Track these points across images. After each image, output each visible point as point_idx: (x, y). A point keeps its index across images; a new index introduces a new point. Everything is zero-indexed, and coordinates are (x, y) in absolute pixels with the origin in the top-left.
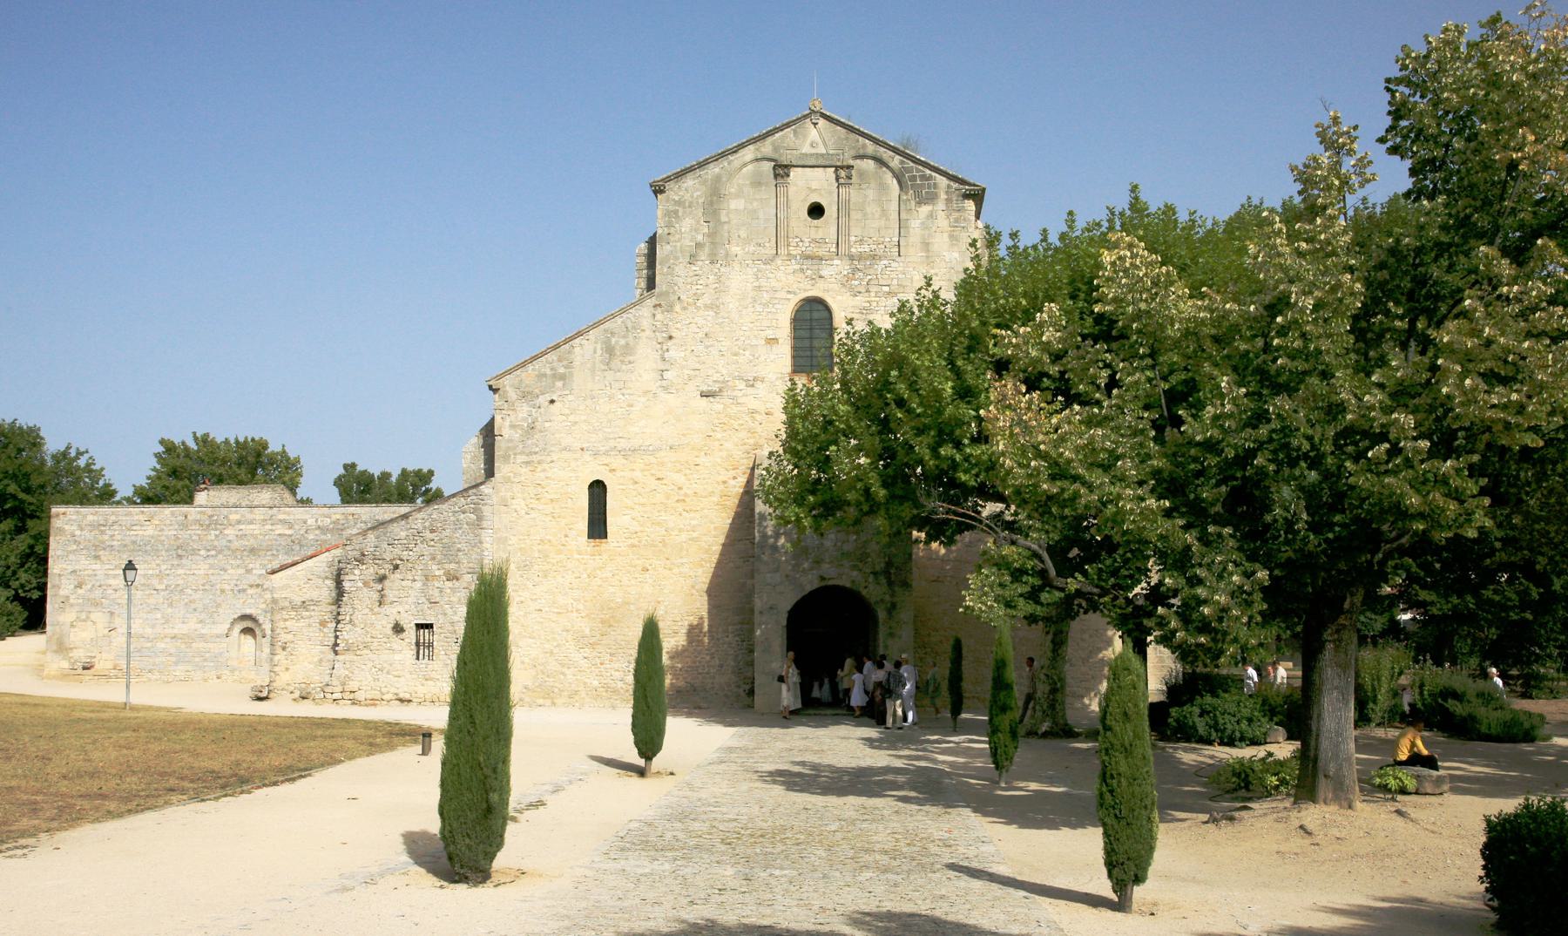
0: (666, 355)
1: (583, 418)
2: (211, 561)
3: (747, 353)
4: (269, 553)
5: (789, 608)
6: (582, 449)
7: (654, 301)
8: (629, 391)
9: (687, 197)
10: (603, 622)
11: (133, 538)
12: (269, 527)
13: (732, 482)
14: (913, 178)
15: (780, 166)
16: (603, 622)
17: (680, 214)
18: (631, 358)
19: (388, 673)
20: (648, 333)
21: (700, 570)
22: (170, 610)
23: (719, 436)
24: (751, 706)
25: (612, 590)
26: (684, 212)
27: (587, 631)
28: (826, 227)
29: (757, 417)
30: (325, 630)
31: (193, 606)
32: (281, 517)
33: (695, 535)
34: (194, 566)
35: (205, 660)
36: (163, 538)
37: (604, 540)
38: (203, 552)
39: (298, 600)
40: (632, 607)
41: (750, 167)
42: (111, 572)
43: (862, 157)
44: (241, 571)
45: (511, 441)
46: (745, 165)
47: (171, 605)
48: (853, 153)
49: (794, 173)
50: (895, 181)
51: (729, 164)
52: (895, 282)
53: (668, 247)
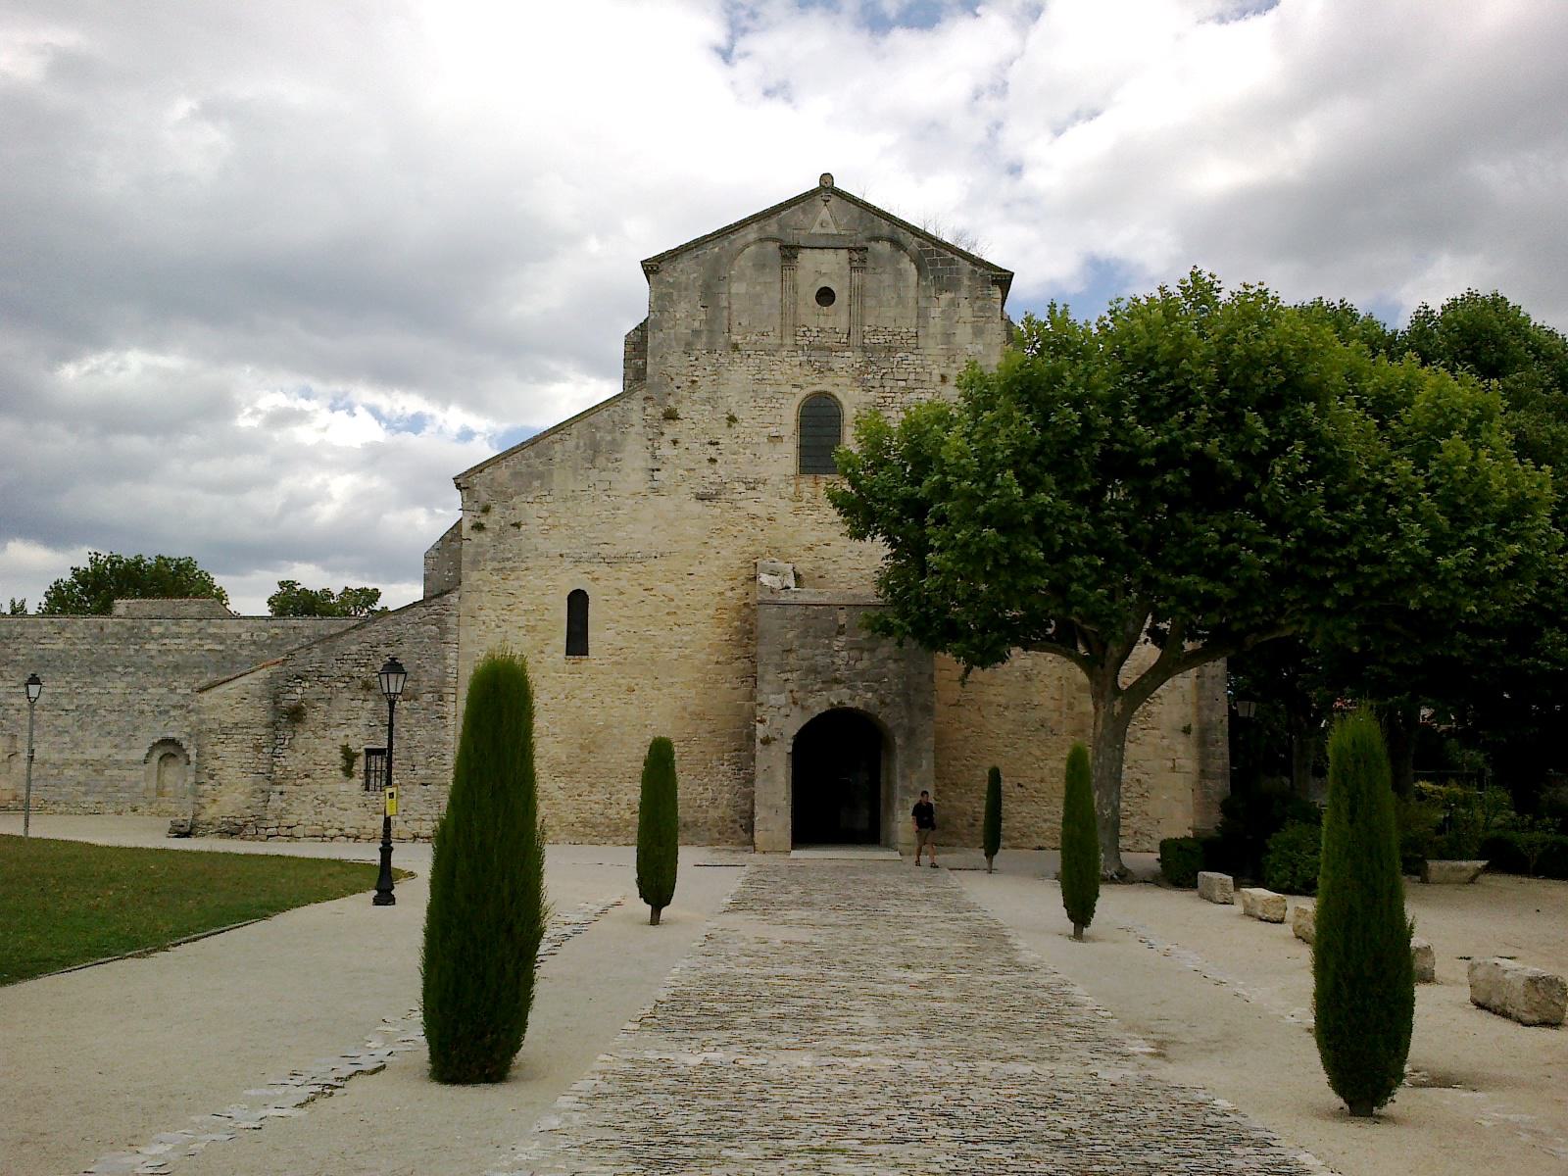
0: (658, 452)
1: (563, 521)
2: (129, 679)
3: (748, 451)
4: (197, 670)
5: (795, 732)
6: (561, 556)
7: (640, 395)
8: (614, 493)
9: (683, 278)
10: (582, 747)
11: (41, 652)
12: (197, 641)
13: (730, 594)
14: (933, 263)
15: (786, 247)
16: (582, 747)
17: (674, 298)
18: (618, 456)
19: (332, 805)
20: (638, 428)
21: (694, 691)
22: (80, 733)
23: (715, 544)
24: (752, 843)
25: (594, 711)
26: (680, 296)
27: (564, 758)
28: (837, 317)
29: (759, 523)
30: (260, 756)
31: (107, 729)
32: (211, 630)
33: (687, 651)
34: (110, 685)
35: (119, 791)
36: (73, 653)
37: (584, 657)
38: (119, 669)
39: (229, 721)
40: (615, 731)
41: (752, 248)
42: (13, 690)
43: (877, 239)
44: (164, 690)
45: (479, 546)
46: (747, 246)
47: (81, 727)
48: (867, 234)
50: (913, 266)
51: (730, 243)
52: (912, 376)
53: (661, 334)
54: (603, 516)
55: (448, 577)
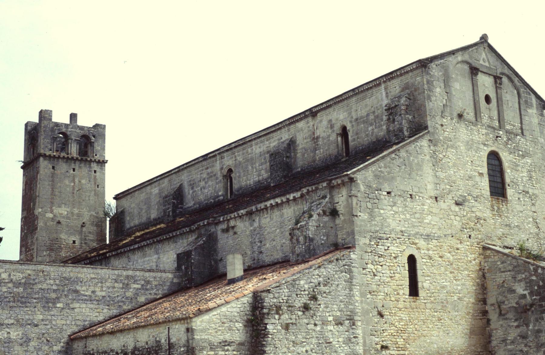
37: (418, 298)
49: (480, 75)
54: (418, 209)
55: (323, 240)
